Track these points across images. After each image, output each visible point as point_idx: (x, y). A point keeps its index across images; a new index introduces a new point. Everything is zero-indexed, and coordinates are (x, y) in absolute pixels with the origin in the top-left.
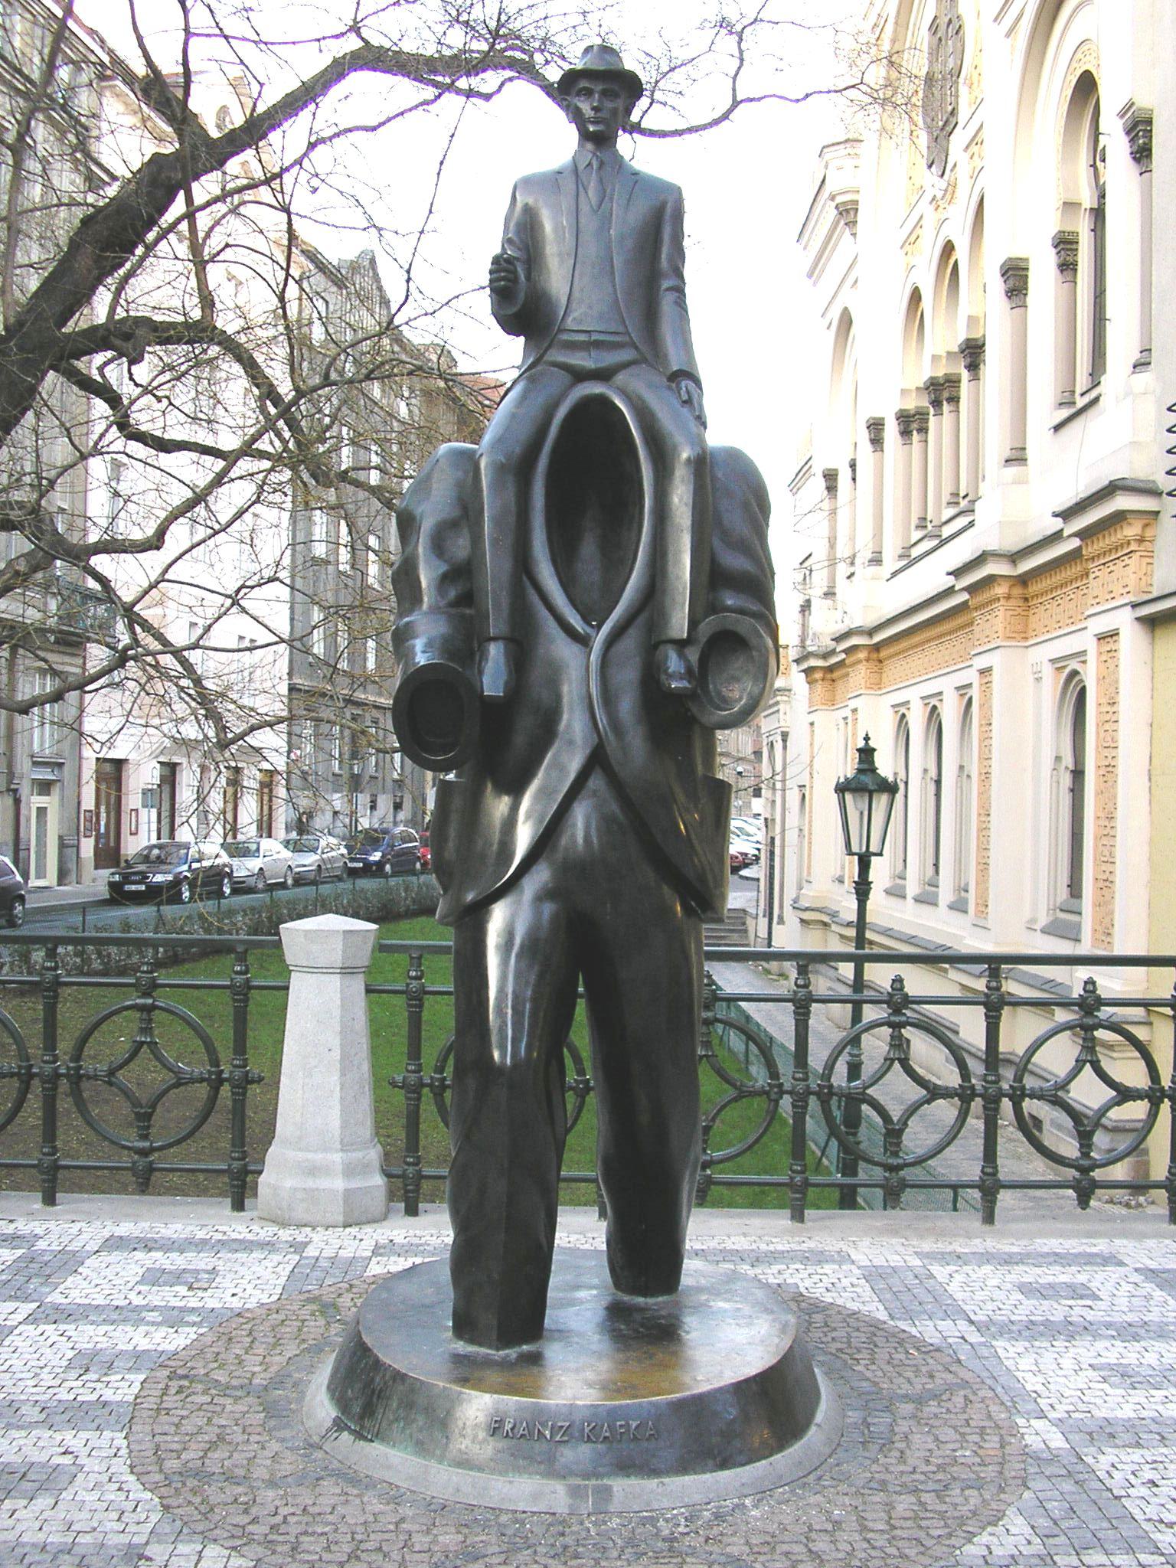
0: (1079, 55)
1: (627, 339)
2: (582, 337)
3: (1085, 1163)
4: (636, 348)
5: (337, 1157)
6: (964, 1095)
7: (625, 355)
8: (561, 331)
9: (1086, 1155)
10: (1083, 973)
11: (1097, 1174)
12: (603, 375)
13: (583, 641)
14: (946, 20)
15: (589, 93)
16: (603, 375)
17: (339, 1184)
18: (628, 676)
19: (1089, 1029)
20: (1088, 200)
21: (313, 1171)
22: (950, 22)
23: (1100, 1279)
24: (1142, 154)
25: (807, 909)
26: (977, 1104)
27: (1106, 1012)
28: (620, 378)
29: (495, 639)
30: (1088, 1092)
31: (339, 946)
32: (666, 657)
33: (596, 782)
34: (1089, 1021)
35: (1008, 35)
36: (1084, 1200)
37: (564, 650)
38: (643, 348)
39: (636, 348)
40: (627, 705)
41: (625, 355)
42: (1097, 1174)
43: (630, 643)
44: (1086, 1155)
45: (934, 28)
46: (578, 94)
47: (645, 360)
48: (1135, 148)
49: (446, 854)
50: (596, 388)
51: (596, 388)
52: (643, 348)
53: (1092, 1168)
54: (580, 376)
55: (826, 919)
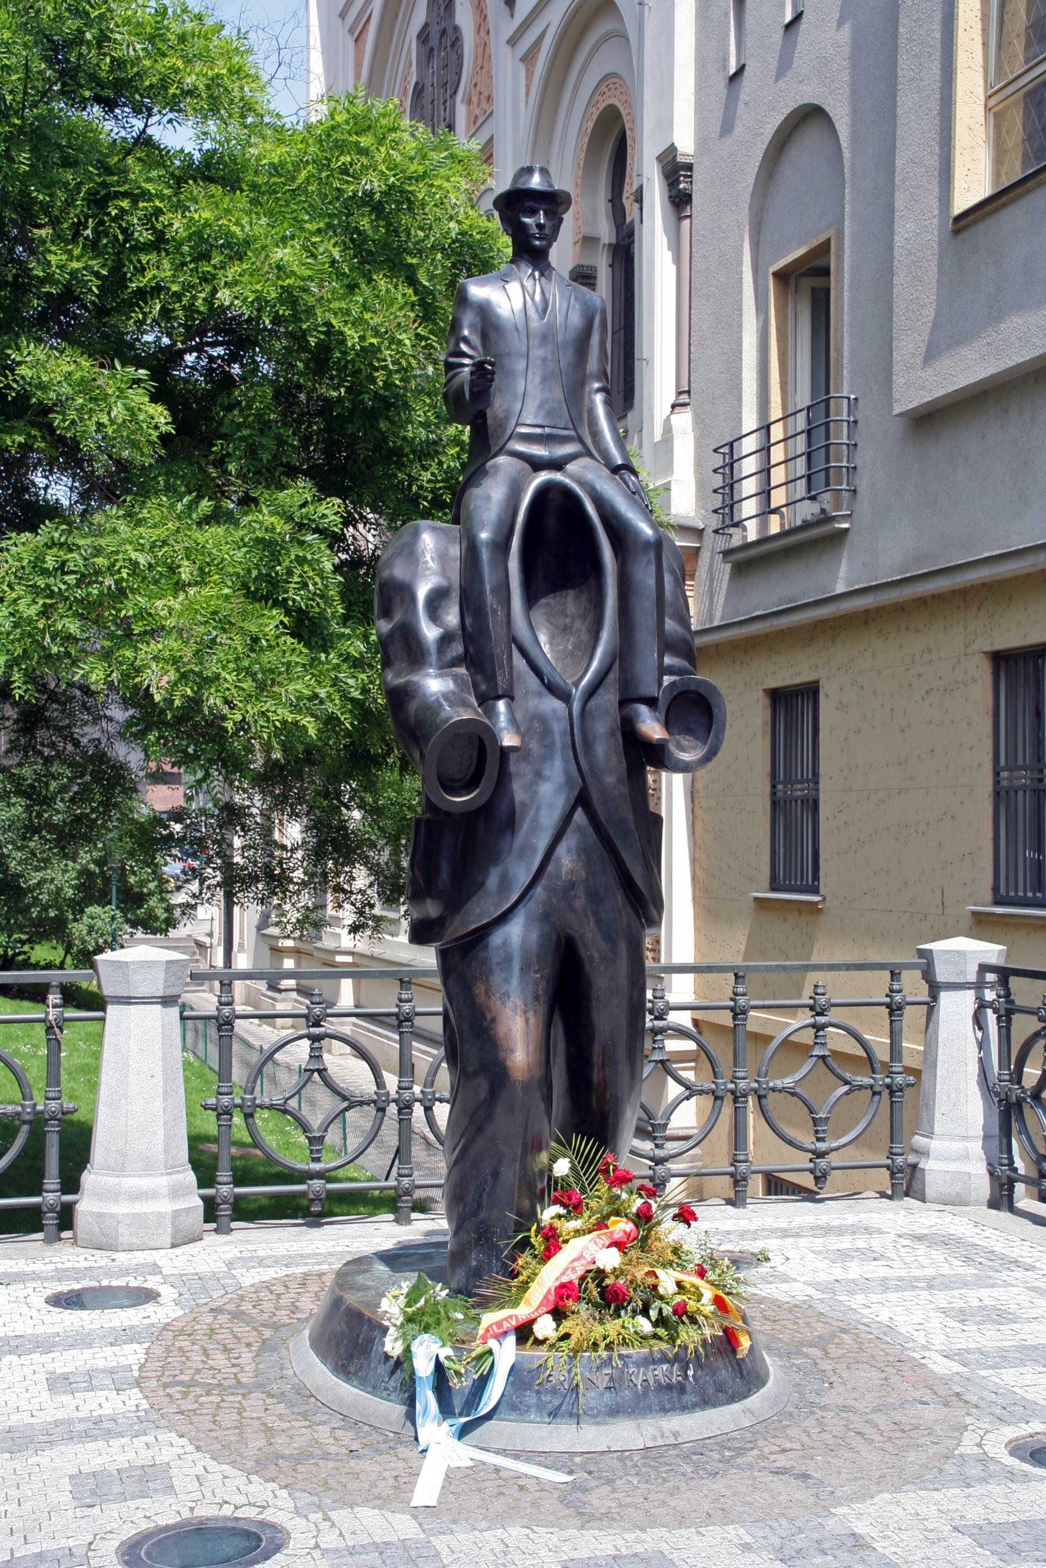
0: (603, 88)
1: (572, 433)
2: (538, 431)
5: (162, 1182)
8: (517, 425)
13: (565, 697)
14: (438, 28)
17: (166, 1206)
19: (818, 1028)
20: (606, 233)
21: (138, 1196)
22: (444, 32)
24: (680, 201)
29: (499, 697)
31: (162, 975)
32: (637, 715)
33: (579, 816)
34: (821, 1020)
35: (523, 59)
39: (581, 441)
45: (423, 36)
47: (589, 454)
48: (674, 193)
50: (558, 476)
51: (558, 476)
52: (589, 441)
54: (537, 465)
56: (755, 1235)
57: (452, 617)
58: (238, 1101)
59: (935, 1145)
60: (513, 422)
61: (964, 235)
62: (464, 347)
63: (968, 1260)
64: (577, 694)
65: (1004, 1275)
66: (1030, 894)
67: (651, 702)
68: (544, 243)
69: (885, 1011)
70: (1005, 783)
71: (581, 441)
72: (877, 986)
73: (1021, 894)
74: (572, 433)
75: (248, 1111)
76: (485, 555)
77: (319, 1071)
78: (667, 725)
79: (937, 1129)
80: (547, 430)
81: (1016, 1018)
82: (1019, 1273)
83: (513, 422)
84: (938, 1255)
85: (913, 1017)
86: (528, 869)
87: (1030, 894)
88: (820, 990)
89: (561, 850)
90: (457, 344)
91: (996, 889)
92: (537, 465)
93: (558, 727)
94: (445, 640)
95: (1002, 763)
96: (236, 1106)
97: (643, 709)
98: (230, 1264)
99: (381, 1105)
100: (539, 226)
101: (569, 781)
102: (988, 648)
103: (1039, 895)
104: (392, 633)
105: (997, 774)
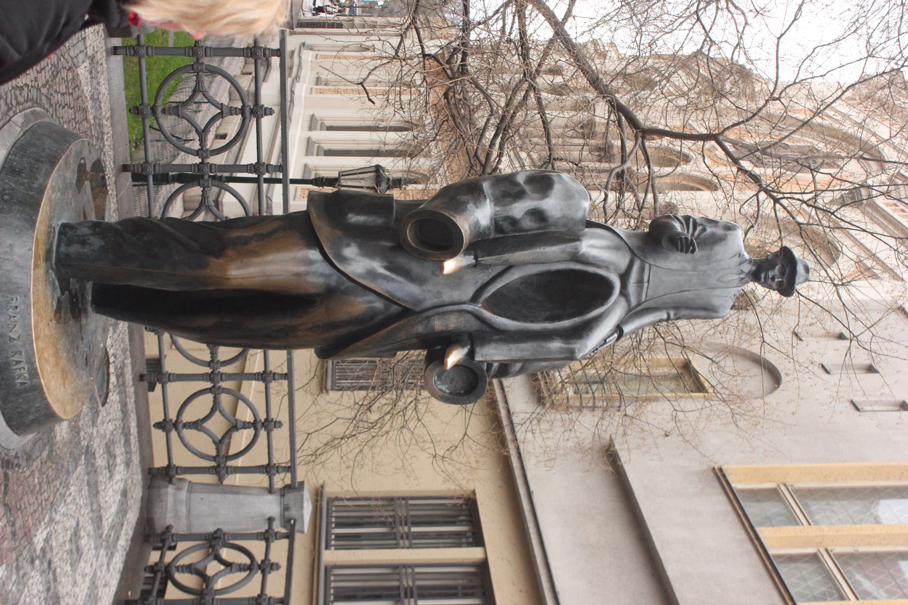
1: (643, 298)
2: (646, 279)
3: (180, 425)
4: (637, 306)
6: (215, 391)
7: (634, 302)
8: (650, 265)
9: (185, 426)
10: (284, 417)
11: (174, 434)
12: (624, 293)
13: (474, 299)
15: (782, 273)
16: (624, 293)
18: (452, 323)
23: (120, 468)
25: (300, 57)
26: (208, 370)
27: (263, 433)
28: (622, 299)
29: (476, 258)
30: (217, 425)
32: (463, 347)
33: (395, 308)
34: (259, 425)
36: (160, 425)
37: (470, 292)
38: (639, 308)
40: (438, 324)
41: (634, 302)
42: (174, 434)
43: (473, 325)
44: (185, 426)
46: (783, 266)
47: (630, 310)
49: (350, 216)
52: (639, 308)
53: (176, 430)
54: (624, 277)
55: (294, 75)
56: (123, 392)
57: (528, 223)
58: (201, 60)
59: (183, 494)
60: (651, 262)
61: (712, 474)
62: (699, 228)
63: (112, 527)
64: (478, 308)
65: (102, 552)
66: (334, 514)
67: (471, 354)
68: (763, 280)
69: (265, 462)
70: (398, 502)
71: (639, 304)
72: (281, 457)
73: (334, 514)
74: (643, 298)
75: (195, 67)
76: (568, 247)
77: (222, 112)
78: (456, 366)
79: (193, 495)
80: (646, 285)
81: (263, 544)
82: (105, 560)
83: (651, 262)
84: (114, 509)
85: (261, 479)
86: (360, 276)
87: (333, 520)
88: (277, 425)
89: (372, 297)
90: (701, 225)
91: (337, 499)
92: (624, 277)
93: (456, 295)
94: (514, 222)
95: (411, 502)
96: (198, 60)
97: (465, 350)
98: (92, 58)
99: (200, 152)
100: (773, 279)
101: (419, 302)
102: (477, 492)
103: (333, 525)
104: (518, 184)
105: (404, 499)
